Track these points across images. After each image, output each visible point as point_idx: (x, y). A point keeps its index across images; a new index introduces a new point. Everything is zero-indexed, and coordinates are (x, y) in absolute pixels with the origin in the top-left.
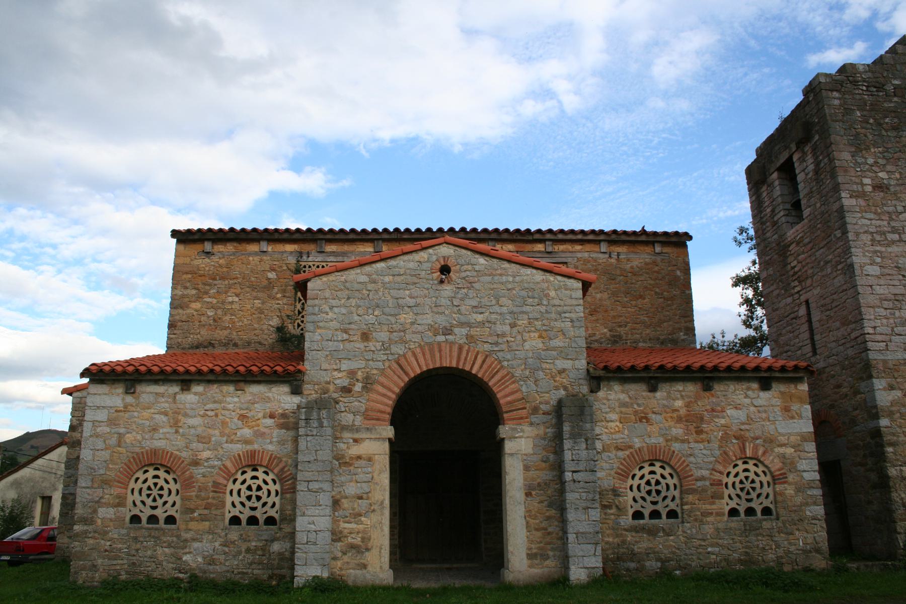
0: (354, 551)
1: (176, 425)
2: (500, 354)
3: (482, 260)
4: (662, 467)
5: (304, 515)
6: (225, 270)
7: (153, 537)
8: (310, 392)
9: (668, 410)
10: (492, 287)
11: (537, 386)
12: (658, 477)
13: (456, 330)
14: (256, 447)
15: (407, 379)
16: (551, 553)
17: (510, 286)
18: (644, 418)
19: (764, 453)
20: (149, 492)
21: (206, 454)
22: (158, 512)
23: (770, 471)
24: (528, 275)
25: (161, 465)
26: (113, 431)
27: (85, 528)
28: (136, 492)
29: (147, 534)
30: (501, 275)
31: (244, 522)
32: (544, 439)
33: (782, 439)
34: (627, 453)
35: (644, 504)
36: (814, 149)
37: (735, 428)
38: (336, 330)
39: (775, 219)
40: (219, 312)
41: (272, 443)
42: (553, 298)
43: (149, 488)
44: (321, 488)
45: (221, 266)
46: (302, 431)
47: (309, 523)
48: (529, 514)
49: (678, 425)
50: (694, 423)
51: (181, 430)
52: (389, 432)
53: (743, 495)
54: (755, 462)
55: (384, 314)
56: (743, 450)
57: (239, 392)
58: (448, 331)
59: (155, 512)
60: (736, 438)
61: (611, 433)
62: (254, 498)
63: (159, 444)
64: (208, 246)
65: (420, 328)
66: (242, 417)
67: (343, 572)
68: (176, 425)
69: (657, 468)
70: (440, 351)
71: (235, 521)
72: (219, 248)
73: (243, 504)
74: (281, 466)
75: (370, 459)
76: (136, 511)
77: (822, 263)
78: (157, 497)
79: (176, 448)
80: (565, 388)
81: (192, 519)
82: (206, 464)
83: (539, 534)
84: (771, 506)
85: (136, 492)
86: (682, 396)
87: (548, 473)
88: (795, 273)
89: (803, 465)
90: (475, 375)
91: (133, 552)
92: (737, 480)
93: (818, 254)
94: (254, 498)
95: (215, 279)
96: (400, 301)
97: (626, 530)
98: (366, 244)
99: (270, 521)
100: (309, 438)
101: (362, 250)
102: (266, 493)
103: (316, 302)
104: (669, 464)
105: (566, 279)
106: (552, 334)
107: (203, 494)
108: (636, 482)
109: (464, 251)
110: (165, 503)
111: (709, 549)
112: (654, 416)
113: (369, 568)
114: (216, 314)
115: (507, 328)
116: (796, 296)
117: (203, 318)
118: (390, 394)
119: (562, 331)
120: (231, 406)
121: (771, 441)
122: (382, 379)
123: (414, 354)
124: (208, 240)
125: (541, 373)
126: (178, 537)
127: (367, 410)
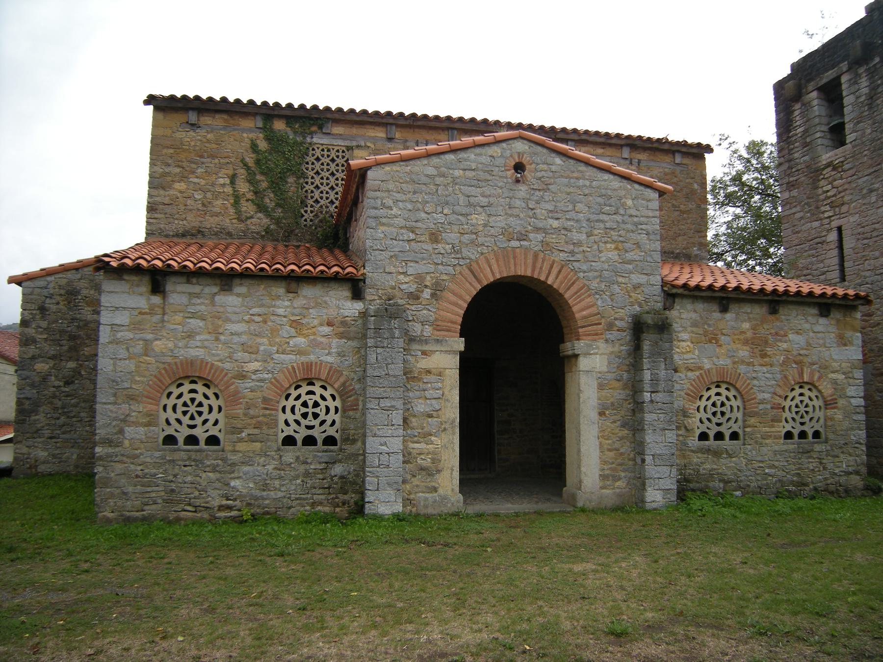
0: (424, 473)
1: (216, 333)
2: (575, 264)
3: (558, 160)
4: (727, 389)
5: (375, 436)
6: (214, 146)
7: (194, 460)
8: (373, 298)
9: (736, 332)
10: (568, 190)
11: (612, 300)
12: (723, 398)
13: (531, 236)
14: (312, 358)
15: (479, 287)
16: (623, 474)
17: (587, 192)
18: (713, 339)
19: (820, 378)
20: (185, 409)
21: (255, 366)
22: (198, 432)
23: (823, 396)
24: (605, 180)
25: (199, 377)
26: (138, 336)
27: (110, 450)
28: (169, 409)
29: (185, 457)
30: (577, 178)
31: (299, 442)
32: (619, 357)
33: (835, 365)
34: (697, 373)
35: (710, 425)
37: (795, 353)
38: (401, 228)
39: (808, 140)
40: (209, 195)
41: (329, 353)
42: (630, 208)
43: (185, 404)
44: (392, 406)
45: (208, 141)
46: (370, 342)
47: (381, 445)
48: (603, 435)
49: (745, 348)
50: (760, 346)
51: (222, 338)
52: (460, 344)
53: (797, 418)
54: (810, 387)
55: (454, 212)
56: (801, 374)
57: (291, 295)
58: (523, 237)
59: (194, 432)
60: (796, 363)
61: (683, 353)
62: (310, 415)
63: (200, 353)
64: (193, 117)
65: (492, 231)
66: (295, 324)
67: (412, 497)
68: (216, 333)
69: (722, 390)
70: (514, 258)
71: (289, 441)
72: (206, 120)
73: (297, 422)
74: (342, 380)
75: (440, 374)
76: (170, 431)
77: (865, 191)
78: (196, 415)
79: (217, 358)
80: (640, 306)
81: (241, 440)
82: (254, 377)
83: (612, 454)
84: (821, 430)
85: (169, 409)
86: (749, 318)
87: (621, 392)
88: (828, 198)
89: (851, 391)
90: (550, 286)
91: (171, 478)
92: (793, 403)
93: (860, 181)
94: (310, 415)
95: (202, 157)
96: (472, 200)
97: (693, 451)
98: (377, 128)
99: (330, 441)
100: (379, 350)
101: (373, 135)
102: (324, 410)
103: (378, 194)
104: (734, 386)
105: (642, 188)
106: (628, 245)
107: (251, 412)
108: (703, 403)
109: (539, 148)
110: (205, 422)
111: (767, 471)
112: (723, 338)
113: (441, 491)
114: (205, 197)
115: (584, 237)
116: (826, 221)
117: (189, 202)
118: (461, 302)
119: (638, 245)
120: (281, 311)
121: (826, 368)
122: (452, 286)
123: (487, 260)
124: (193, 109)
125: (616, 286)
126: (224, 460)
127: (436, 320)
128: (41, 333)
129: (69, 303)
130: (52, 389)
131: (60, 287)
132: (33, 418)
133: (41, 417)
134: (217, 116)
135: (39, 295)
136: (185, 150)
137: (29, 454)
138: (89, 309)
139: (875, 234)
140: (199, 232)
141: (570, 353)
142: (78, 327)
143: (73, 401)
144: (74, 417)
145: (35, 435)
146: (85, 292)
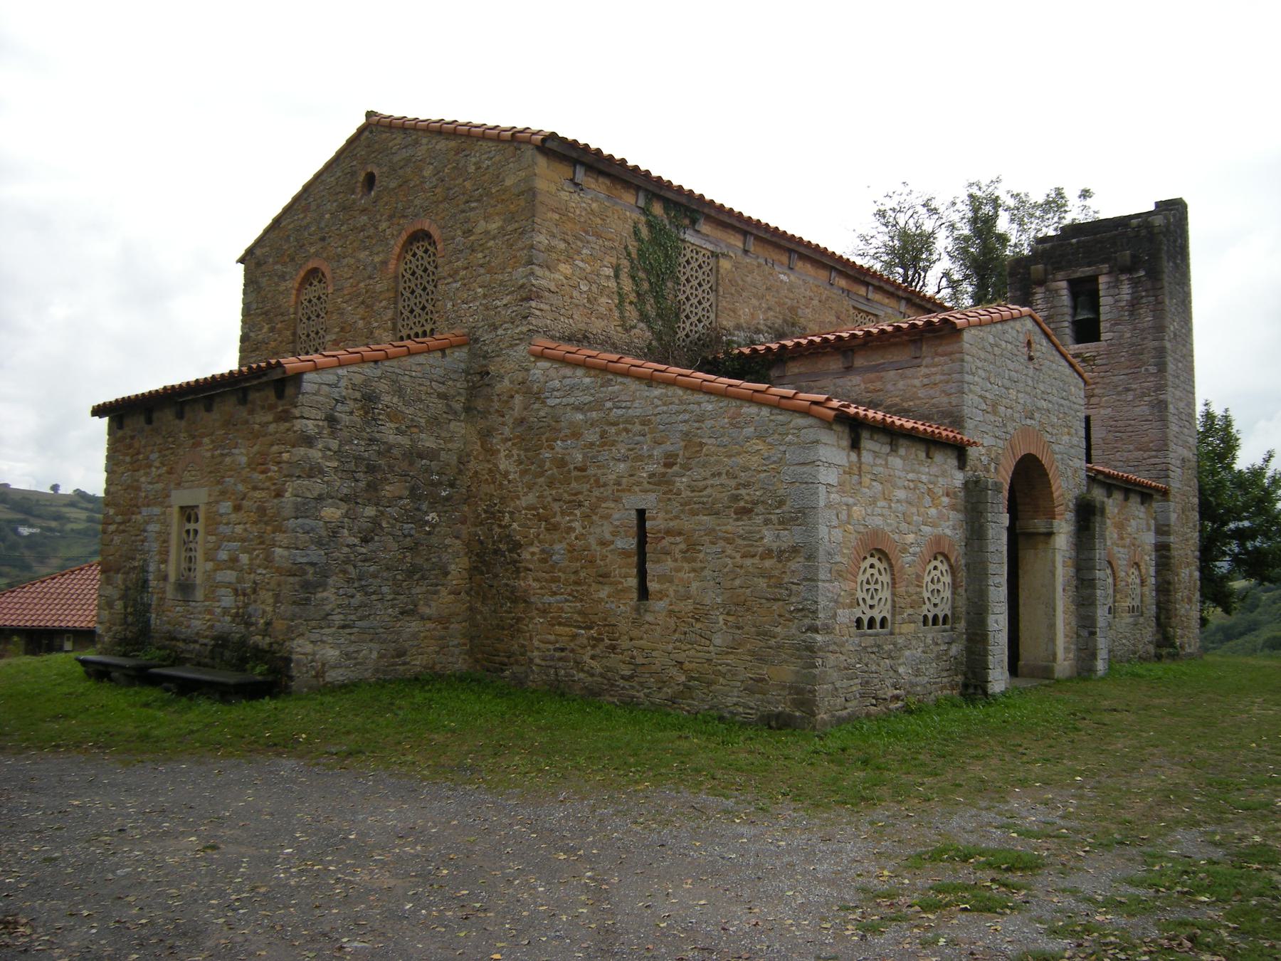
36: (1135, 284)
64: (580, 175)
93: (1115, 379)
128: (330, 459)
129: (366, 413)
130: (346, 550)
131: (354, 387)
132: (319, 595)
133: (329, 594)
134: (601, 180)
135: (327, 396)
136: (570, 219)
137: (314, 654)
138: (392, 425)
139: (1130, 429)
140: (585, 337)
141: (1042, 530)
142: (379, 453)
143: (372, 569)
144: (374, 593)
145: (323, 624)
146: (386, 399)
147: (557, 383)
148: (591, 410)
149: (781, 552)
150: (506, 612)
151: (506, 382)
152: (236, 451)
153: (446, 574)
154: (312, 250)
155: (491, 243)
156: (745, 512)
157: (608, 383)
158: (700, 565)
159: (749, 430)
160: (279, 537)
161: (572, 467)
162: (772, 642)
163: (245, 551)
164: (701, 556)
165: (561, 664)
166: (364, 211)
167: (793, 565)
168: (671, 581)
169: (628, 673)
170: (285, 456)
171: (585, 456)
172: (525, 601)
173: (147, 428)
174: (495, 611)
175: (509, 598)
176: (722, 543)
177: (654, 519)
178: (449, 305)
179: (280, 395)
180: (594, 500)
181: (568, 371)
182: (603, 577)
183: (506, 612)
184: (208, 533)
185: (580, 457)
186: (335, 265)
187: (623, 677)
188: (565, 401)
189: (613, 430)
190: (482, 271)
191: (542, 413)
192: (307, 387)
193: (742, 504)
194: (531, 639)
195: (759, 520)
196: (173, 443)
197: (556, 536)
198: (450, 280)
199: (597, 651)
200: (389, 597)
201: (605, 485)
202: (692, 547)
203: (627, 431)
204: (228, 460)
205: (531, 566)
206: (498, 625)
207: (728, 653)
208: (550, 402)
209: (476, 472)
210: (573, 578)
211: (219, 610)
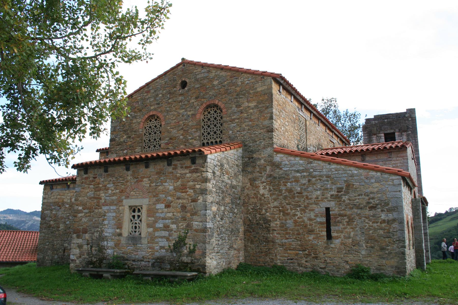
36: (408, 135)
130: (218, 223)
134: (284, 91)
138: (227, 176)
146: (225, 165)
147: (287, 163)
148: (303, 172)
149: (388, 222)
150: (263, 246)
151: (262, 161)
152: (166, 184)
153: (239, 232)
154: (152, 108)
155: (251, 111)
156: (372, 208)
157: (311, 163)
158: (354, 226)
159: (373, 181)
160: (195, 217)
161: (295, 192)
162: (387, 252)
163: (173, 223)
164: (355, 223)
165: (291, 265)
166: (181, 95)
167: (394, 225)
168: (342, 232)
169: (324, 266)
170: (198, 186)
171: (301, 189)
172: (273, 242)
173: (104, 173)
174: (258, 246)
175: (264, 241)
176: (363, 218)
177: (334, 211)
178: (230, 132)
179: (193, 162)
180: (306, 204)
181: (292, 158)
182: (311, 232)
183: (263, 246)
184: (148, 216)
185: (299, 189)
186: (166, 114)
187: (321, 268)
188: (291, 169)
189: (314, 179)
190: (247, 120)
191: (280, 173)
192: (209, 160)
193: (371, 205)
194: (276, 255)
195: (379, 210)
196: (123, 180)
197: (288, 217)
198: (230, 123)
199: (308, 259)
200: (227, 241)
201: (311, 199)
202: (351, 220)
203: (320, 180)
204: (161, 188)
205: (276, 229)
206: (259, 252)
207: (368, 257)
208: (285, 169)
209: (248, 195)
210: (296, 232)
211: (158, 247)
